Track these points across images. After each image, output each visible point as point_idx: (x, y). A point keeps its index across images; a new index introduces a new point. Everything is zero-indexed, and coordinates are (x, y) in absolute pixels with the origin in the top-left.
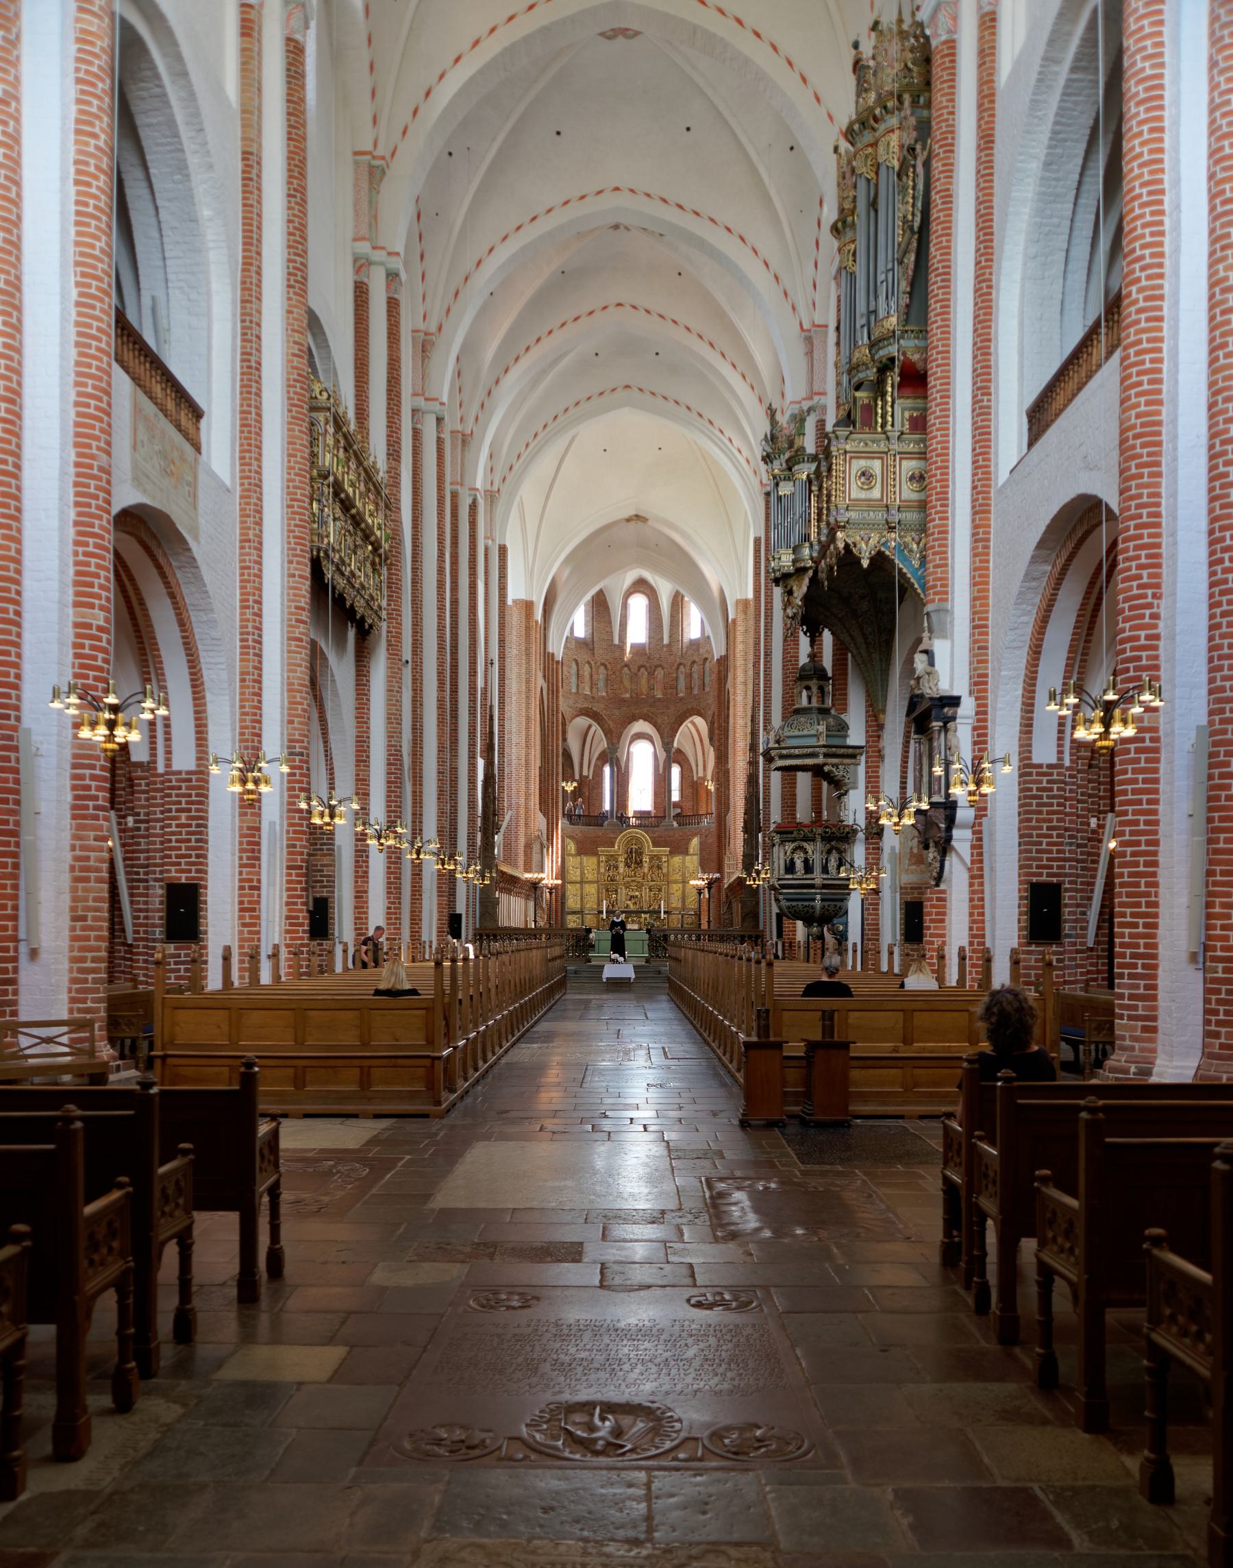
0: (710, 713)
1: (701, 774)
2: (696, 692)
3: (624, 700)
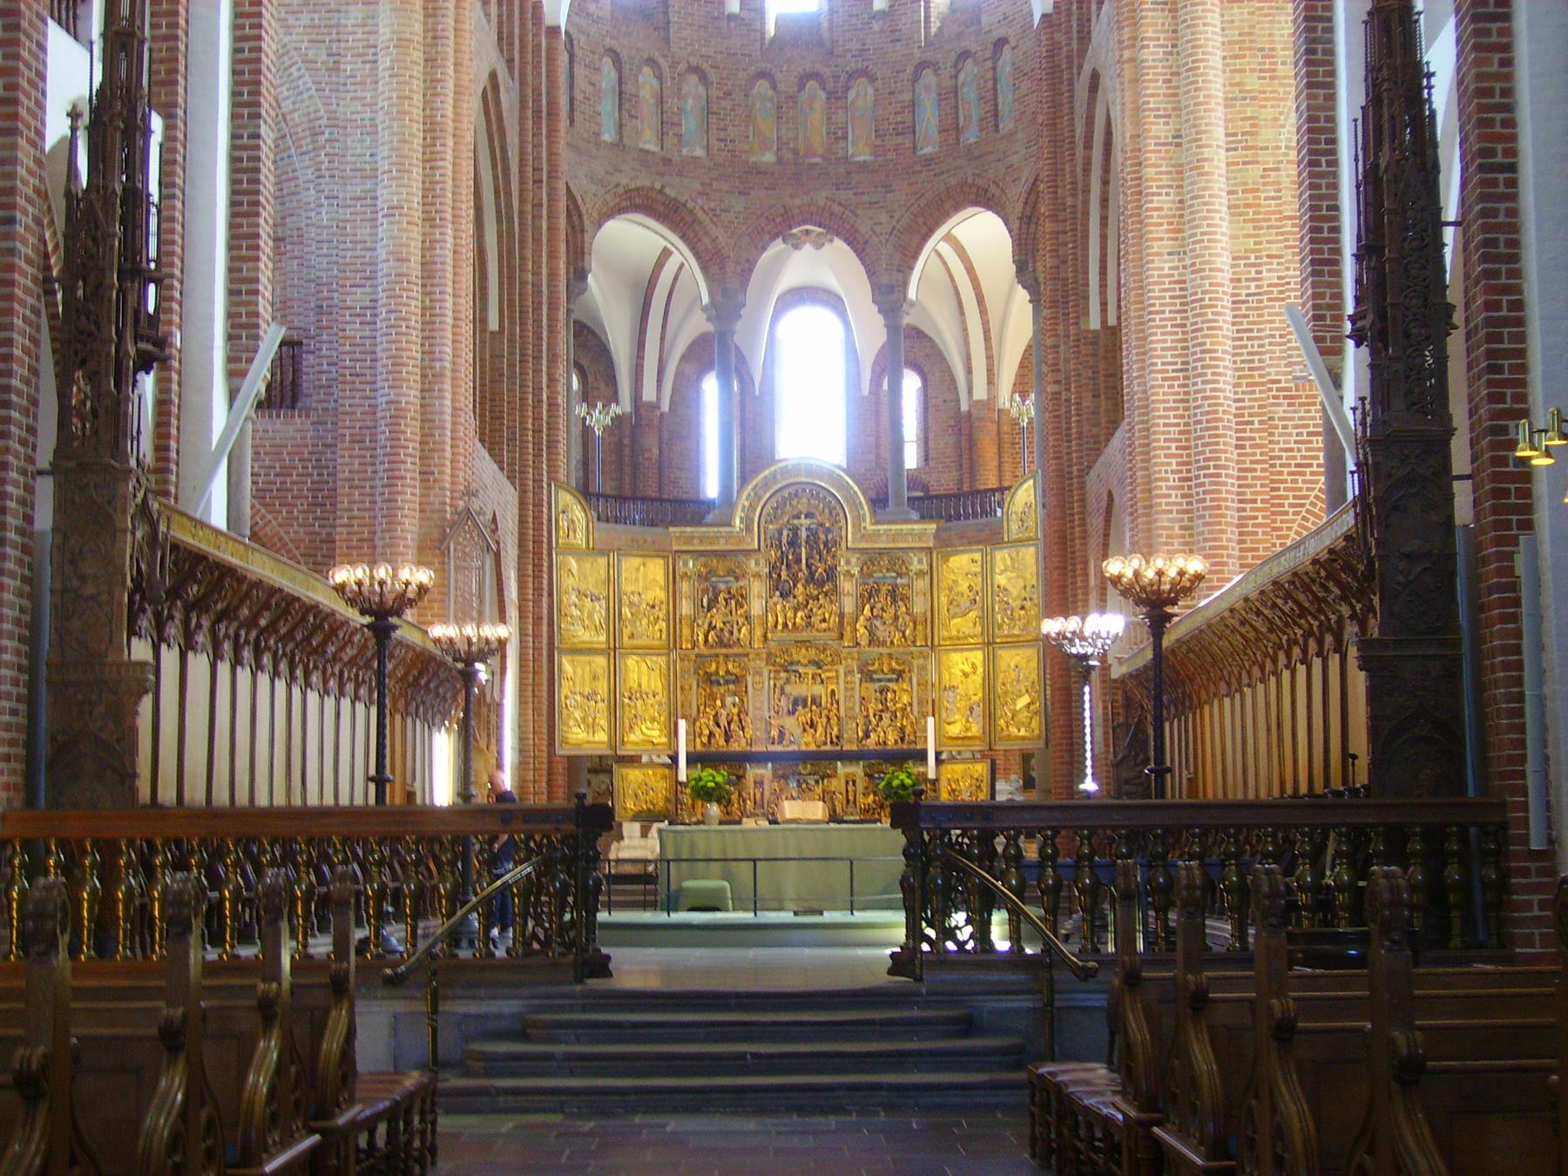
0: (1017, 192)
1: (980, 393)
2: (971, 136)
3: (759, 171)
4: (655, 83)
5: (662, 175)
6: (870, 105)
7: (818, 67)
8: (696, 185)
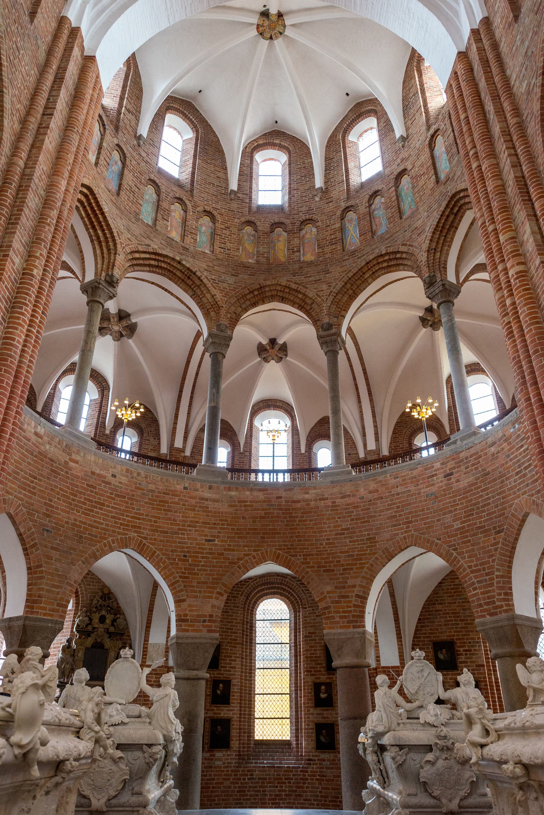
1: (372, 445)
3: (246, 266)
4: (182, 212)
5: (181, 254)
6: (313, 236)
7: (283, 220)
8: (204, 265)
